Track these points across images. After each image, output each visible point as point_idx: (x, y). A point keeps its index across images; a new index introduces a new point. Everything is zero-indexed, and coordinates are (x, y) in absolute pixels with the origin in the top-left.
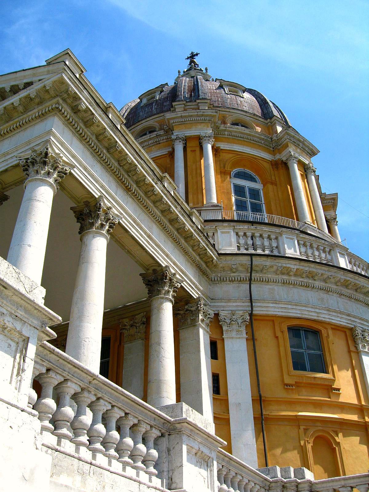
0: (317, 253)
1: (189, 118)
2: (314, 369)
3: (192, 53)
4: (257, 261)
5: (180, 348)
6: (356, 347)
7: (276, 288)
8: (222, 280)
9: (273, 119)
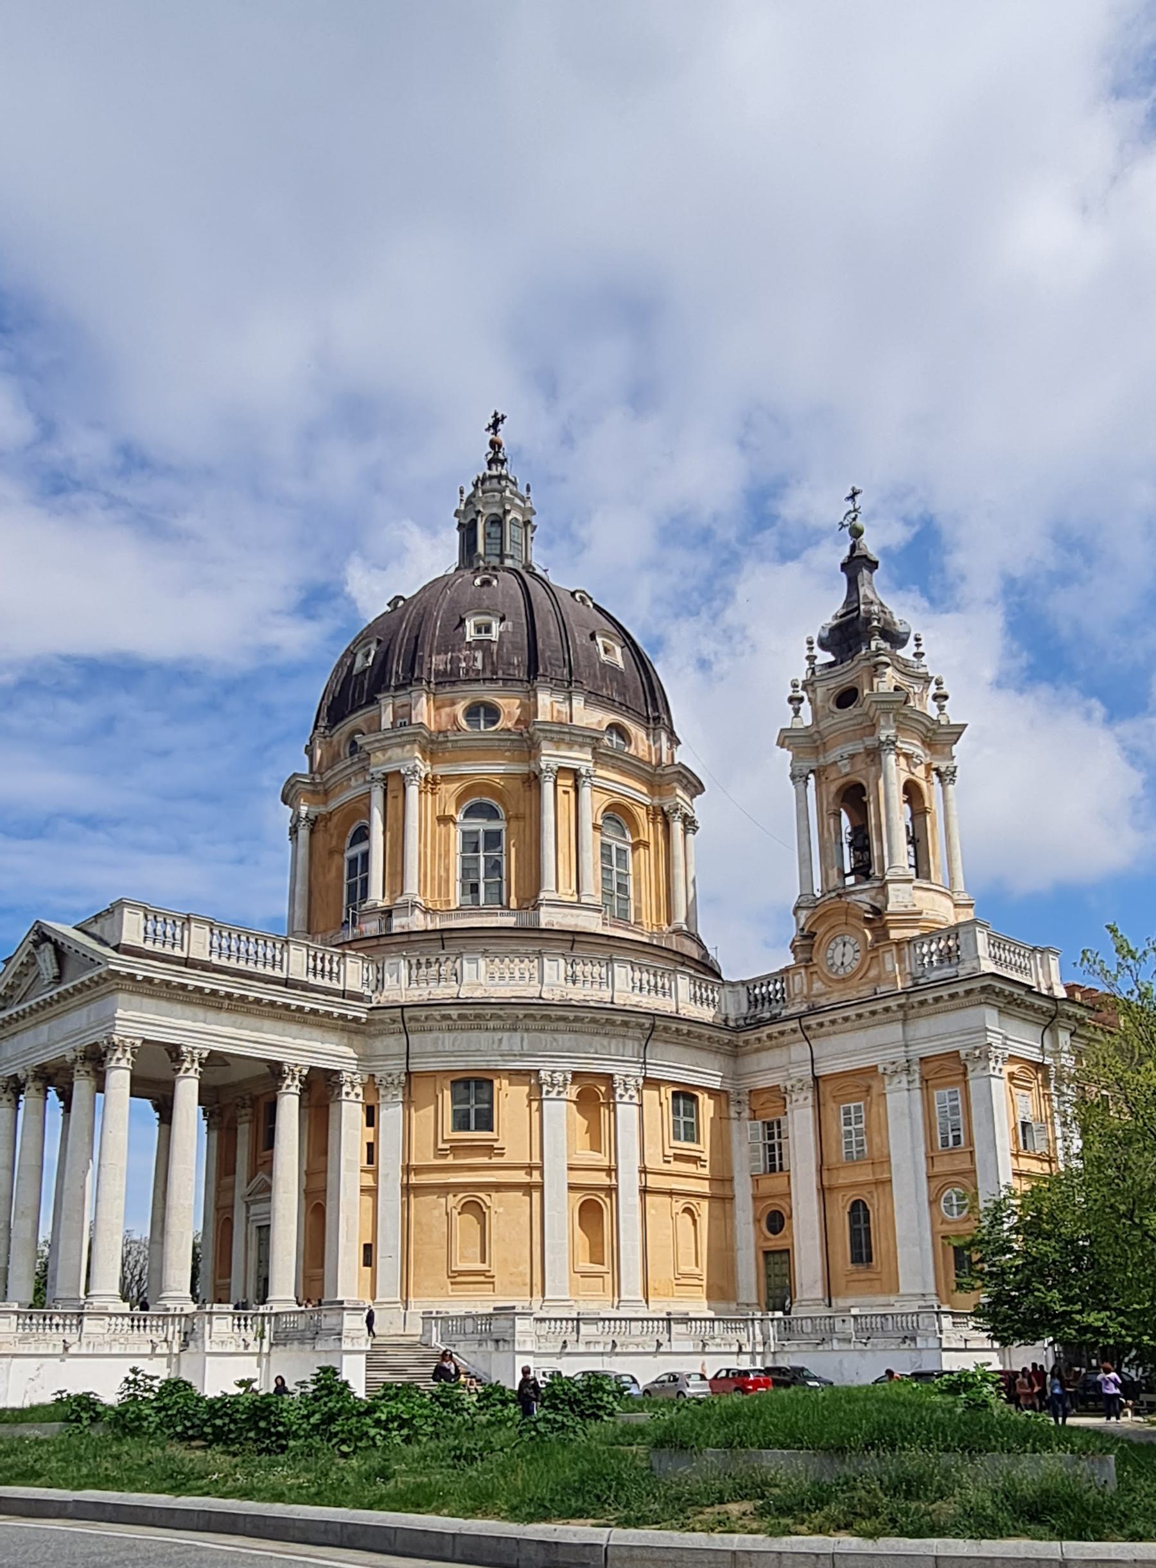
2: (477, 1129)
3: (496, 414)
4: (408, 1013)
6: (541, 1093)
7: (441, 1035)
8: (381, 1034)
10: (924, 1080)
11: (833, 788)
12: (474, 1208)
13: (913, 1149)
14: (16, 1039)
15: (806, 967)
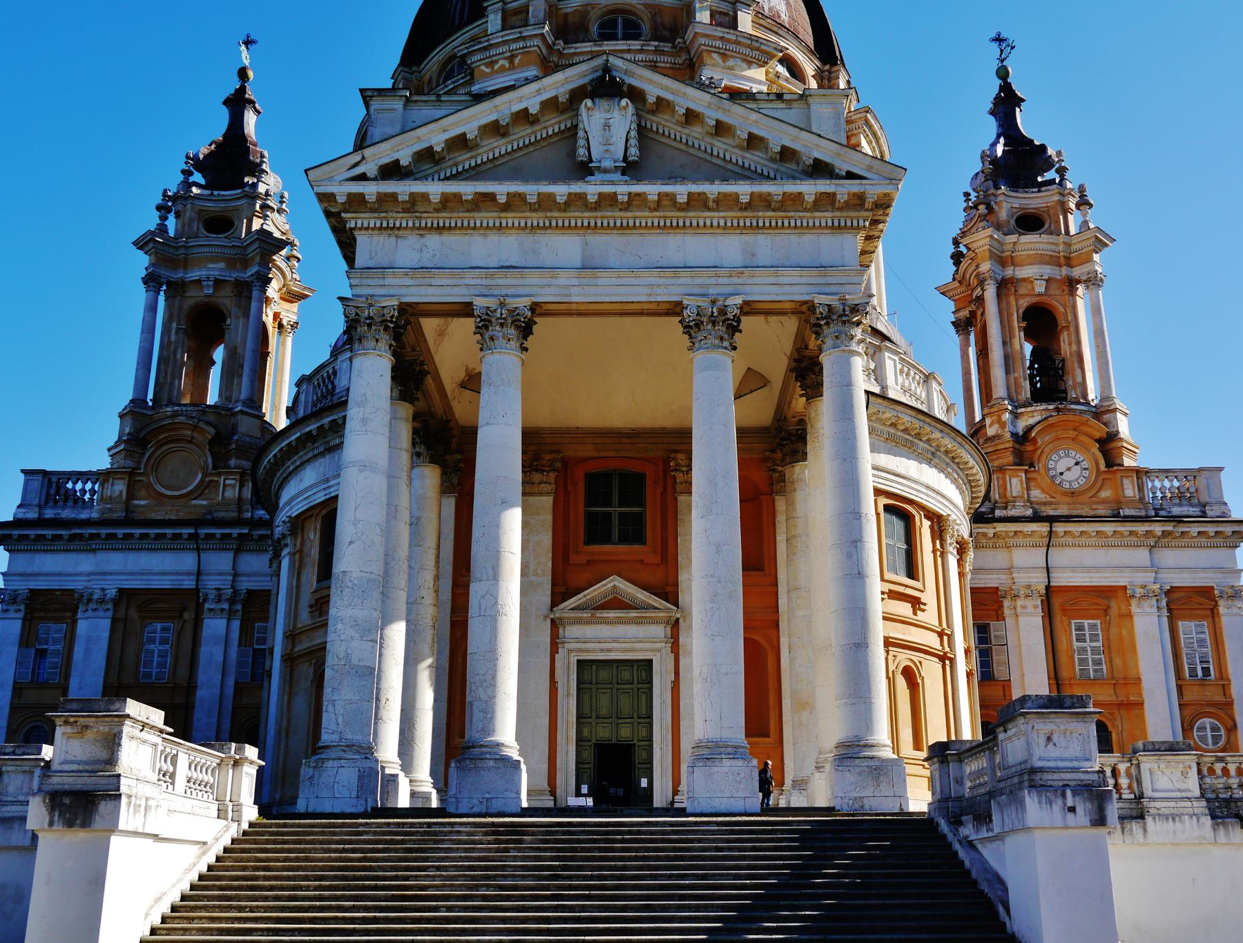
0: (918, 392)
1: (734, 46)
5: (777, 524)
9: (835, 68)
10: (1170, 610)
11: (1024, 303)
12: (909, 674)
13: (1166, 674)
14: (448, 238)
15: (1026, 472)
